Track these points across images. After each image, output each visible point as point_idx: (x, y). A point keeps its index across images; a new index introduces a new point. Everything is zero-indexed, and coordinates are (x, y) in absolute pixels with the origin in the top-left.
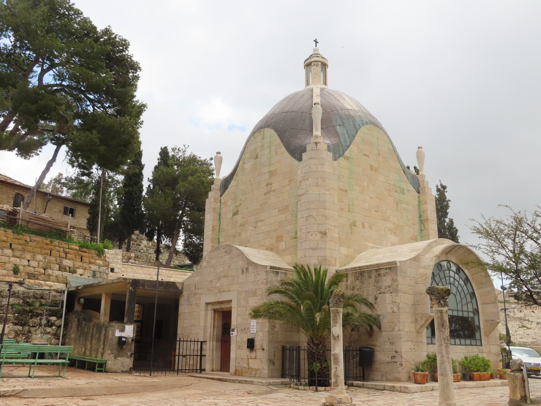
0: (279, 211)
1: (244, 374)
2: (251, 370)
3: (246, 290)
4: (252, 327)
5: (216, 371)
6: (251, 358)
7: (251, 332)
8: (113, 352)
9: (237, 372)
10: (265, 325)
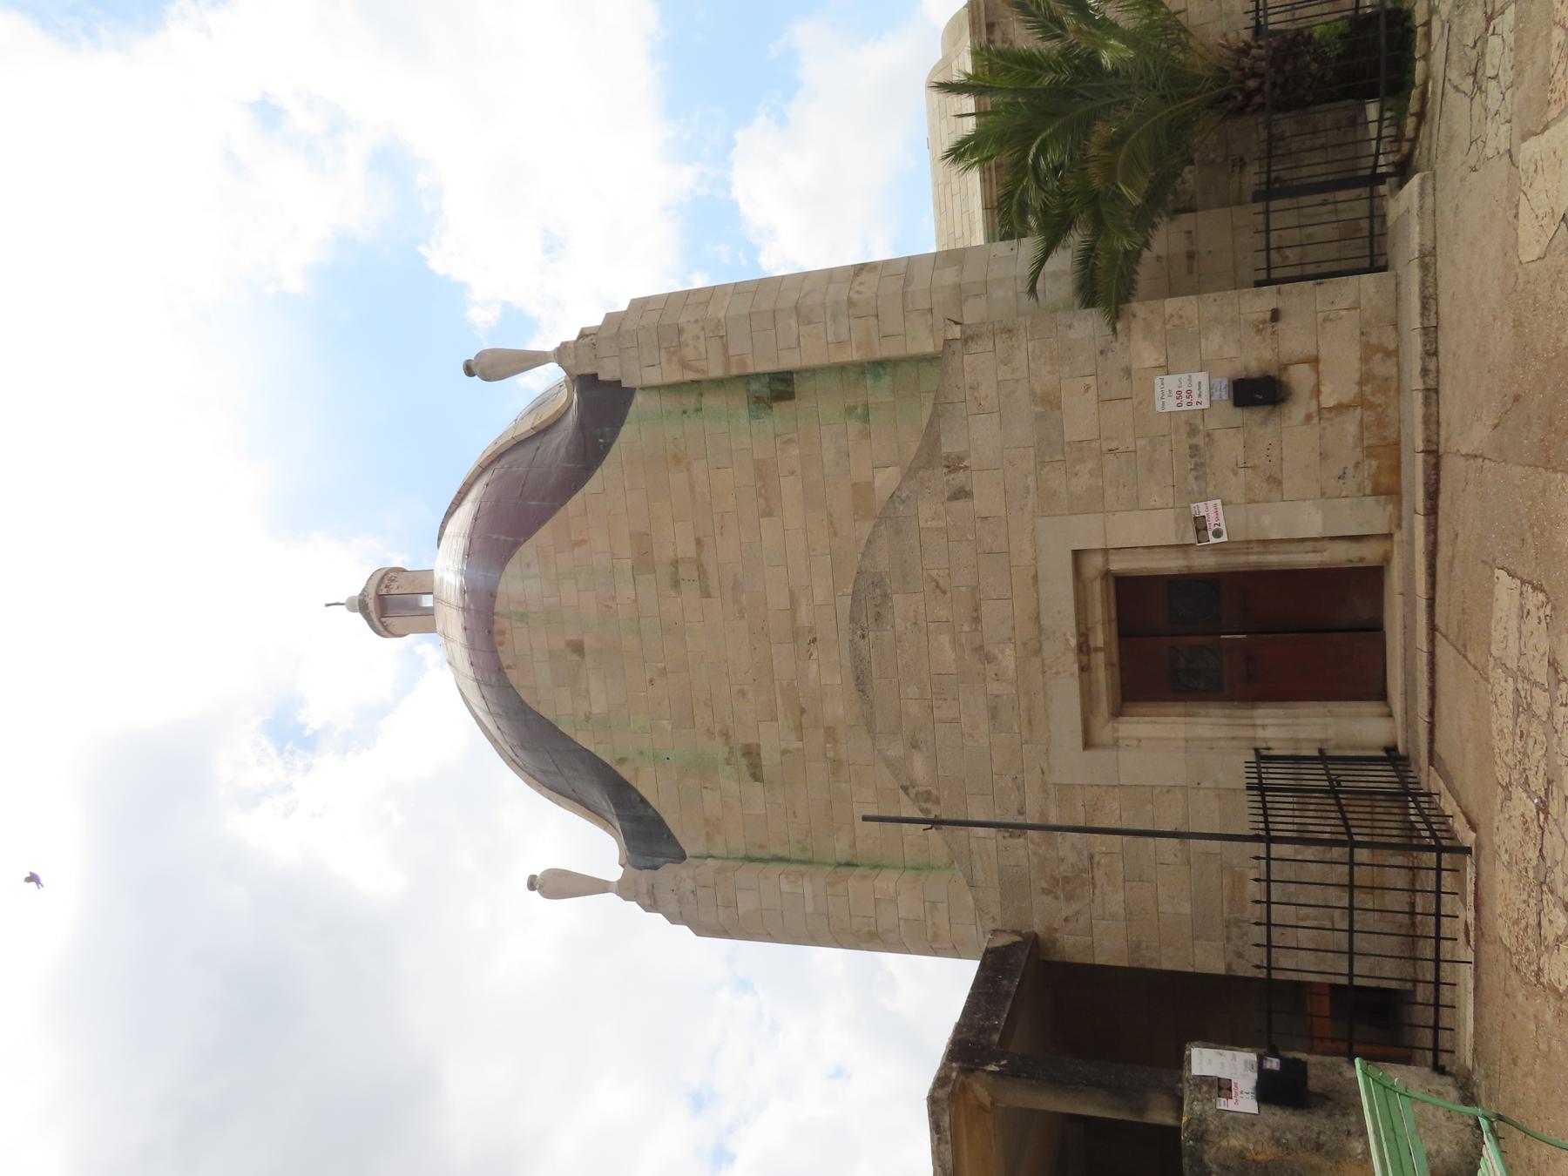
0: (768, 513)
1: (1391, 435)
2: (1368, 389)
3: (1032, 464)
4: (1185, 401)
5: (1388, 705)
6: (1317, 392)
7: (1206, 405)
8: (1353, 1129)
9: (1385, 480)
10: (1175, 321)
